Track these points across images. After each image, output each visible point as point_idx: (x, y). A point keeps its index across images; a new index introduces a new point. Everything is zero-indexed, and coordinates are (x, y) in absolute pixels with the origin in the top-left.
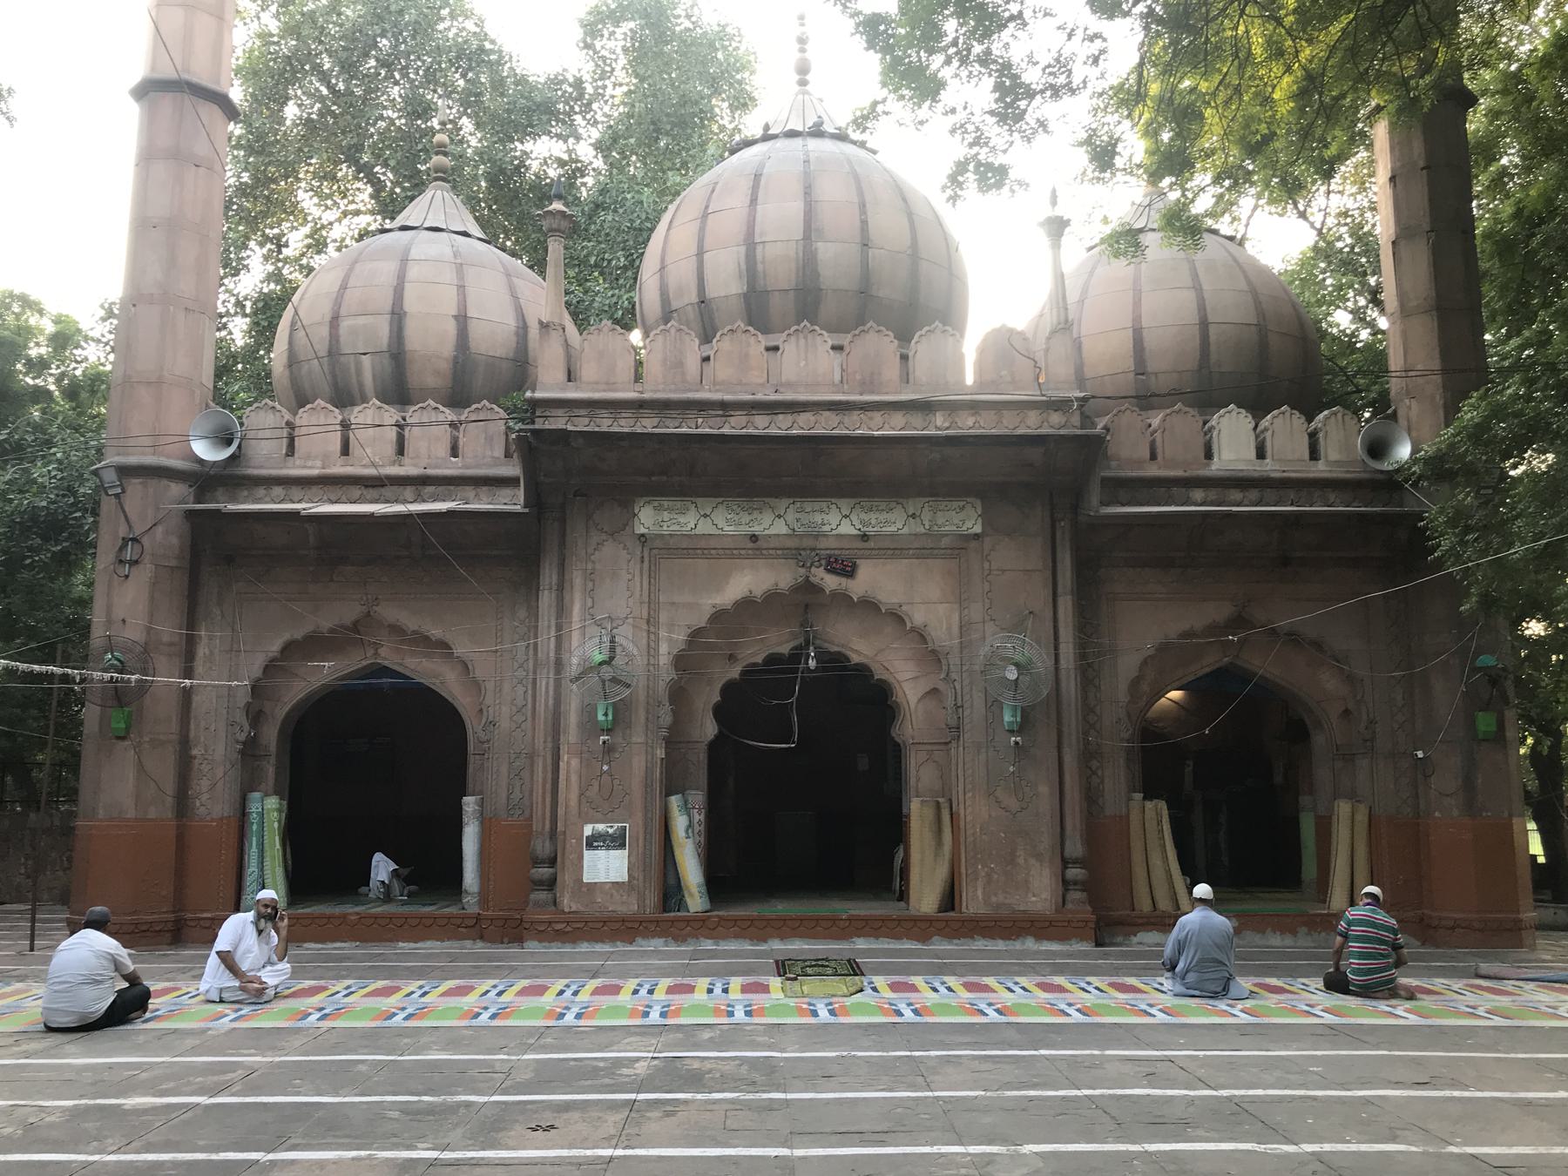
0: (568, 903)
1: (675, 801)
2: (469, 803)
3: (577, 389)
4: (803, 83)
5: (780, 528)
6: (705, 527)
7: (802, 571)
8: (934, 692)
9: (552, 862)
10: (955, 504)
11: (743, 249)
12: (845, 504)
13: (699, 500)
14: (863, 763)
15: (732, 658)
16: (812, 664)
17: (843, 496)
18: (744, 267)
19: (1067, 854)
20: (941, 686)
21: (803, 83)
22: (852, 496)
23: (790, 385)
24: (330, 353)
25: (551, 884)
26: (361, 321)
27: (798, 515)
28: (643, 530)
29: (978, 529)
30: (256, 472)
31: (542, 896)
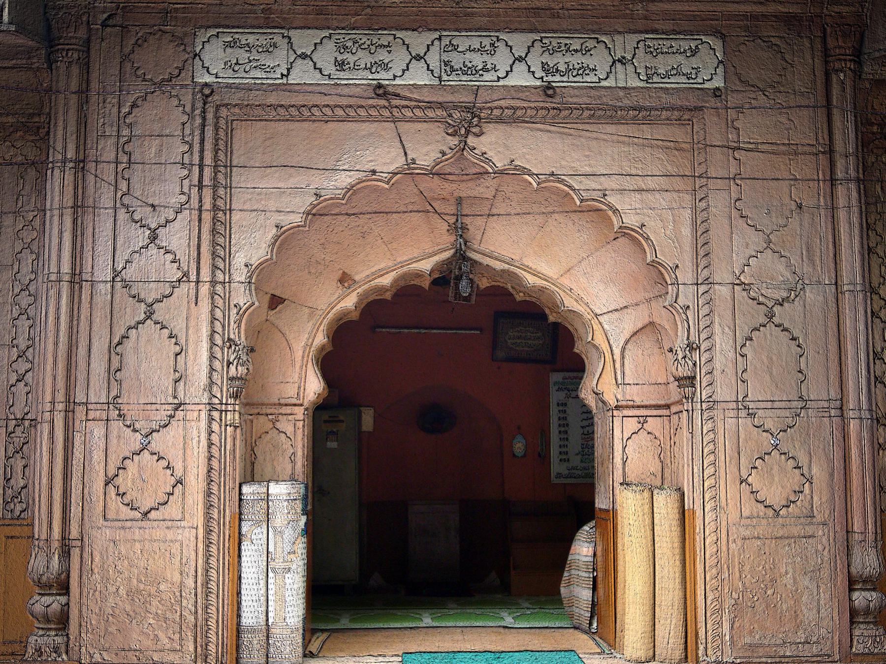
5: (418, 76)
6: (303, 74)
7: (454, 141)
10: (685, 45)
14: (519, 446)
15: (345, 279)
19: (854, 571)
20: (662, 318)
25: (62, 621)
28: (208, 79)
29: (718, 82)
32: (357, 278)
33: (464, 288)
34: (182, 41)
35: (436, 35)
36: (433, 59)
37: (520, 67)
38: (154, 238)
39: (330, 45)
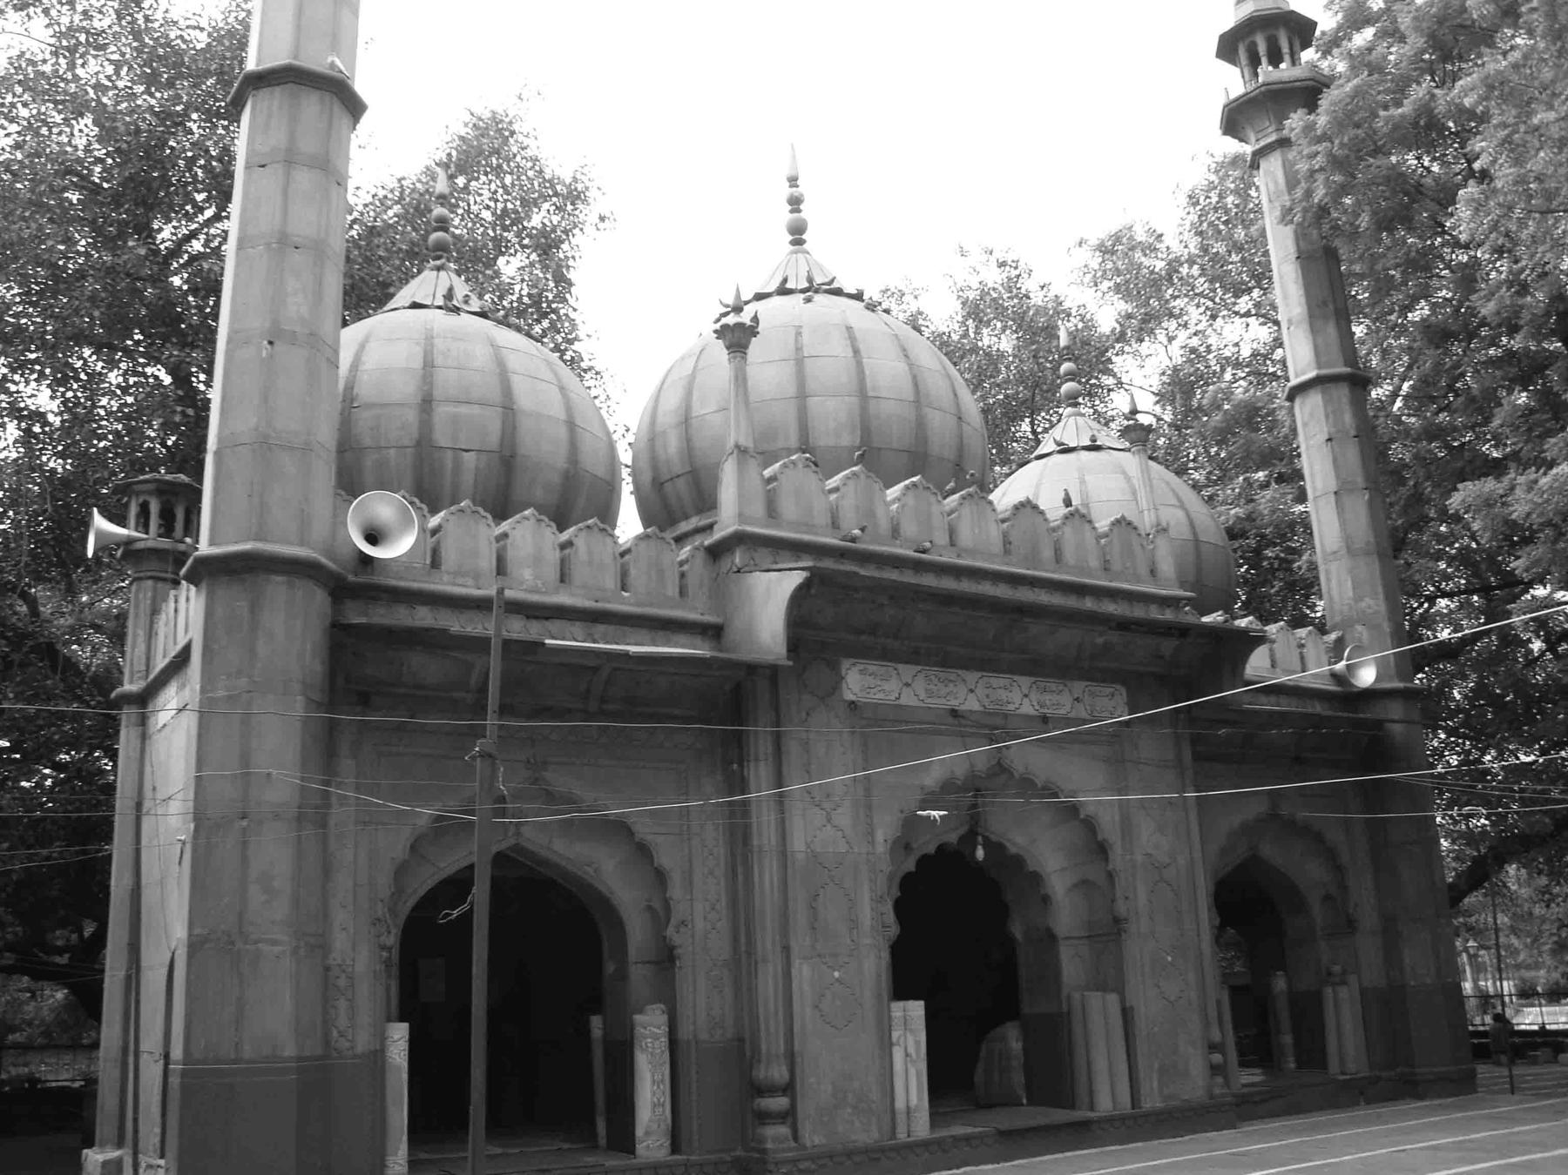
0: (813, 1137)
1: (898, 1008)
2: (650, 1028)
3: (778, 526)
4: (798, 242)
5: (972, 704)
6: (908, 699)
8: (1084, 884)
9: (789, 1089)
11: (855, 400)
12: (1025, 681)
13: (900, 666)
16: (980, 853)
17: (1022, 674)
18: (858, 419)
21: (798, 242)
22: (1030, 674)
23: (972, 552)
24: (419, 444)
26: (463, 410)
27: (987, 691)
30: (393, 582)
31: (783, 1130)
32: (915, 846)
33: (980, 853)
34: (834, 667)
35: (980, 674)
36: (980, 691)
37: (1026, 700)
38: (829, 821)
39: (921, 676)
